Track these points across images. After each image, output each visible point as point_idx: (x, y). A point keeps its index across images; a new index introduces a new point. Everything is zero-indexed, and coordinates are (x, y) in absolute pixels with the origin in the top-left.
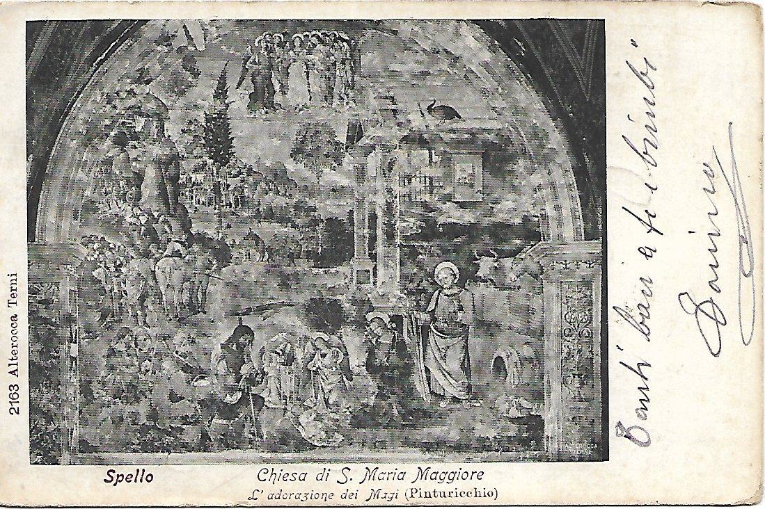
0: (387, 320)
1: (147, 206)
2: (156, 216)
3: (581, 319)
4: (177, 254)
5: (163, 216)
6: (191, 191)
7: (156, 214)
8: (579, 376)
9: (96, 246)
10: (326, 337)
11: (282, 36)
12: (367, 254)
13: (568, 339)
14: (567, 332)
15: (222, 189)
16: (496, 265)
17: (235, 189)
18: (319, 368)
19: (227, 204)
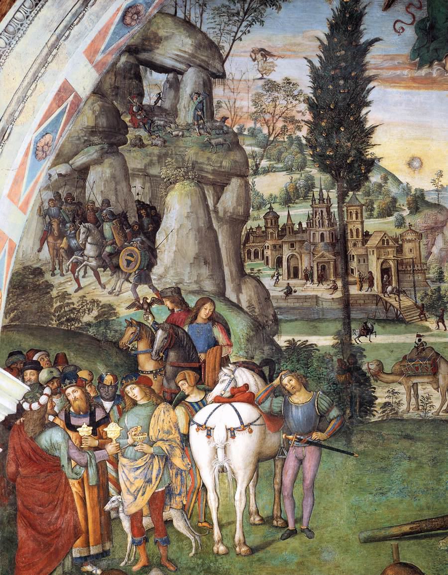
1: (170, 281)
2: (192, 305)
4: (240, 394)
5: (208, 306)
6: (277, 248)
7: (192, 301)
9: (44, 375)
15: (350, 245)
17: (384, 242)
19: (362, 280)
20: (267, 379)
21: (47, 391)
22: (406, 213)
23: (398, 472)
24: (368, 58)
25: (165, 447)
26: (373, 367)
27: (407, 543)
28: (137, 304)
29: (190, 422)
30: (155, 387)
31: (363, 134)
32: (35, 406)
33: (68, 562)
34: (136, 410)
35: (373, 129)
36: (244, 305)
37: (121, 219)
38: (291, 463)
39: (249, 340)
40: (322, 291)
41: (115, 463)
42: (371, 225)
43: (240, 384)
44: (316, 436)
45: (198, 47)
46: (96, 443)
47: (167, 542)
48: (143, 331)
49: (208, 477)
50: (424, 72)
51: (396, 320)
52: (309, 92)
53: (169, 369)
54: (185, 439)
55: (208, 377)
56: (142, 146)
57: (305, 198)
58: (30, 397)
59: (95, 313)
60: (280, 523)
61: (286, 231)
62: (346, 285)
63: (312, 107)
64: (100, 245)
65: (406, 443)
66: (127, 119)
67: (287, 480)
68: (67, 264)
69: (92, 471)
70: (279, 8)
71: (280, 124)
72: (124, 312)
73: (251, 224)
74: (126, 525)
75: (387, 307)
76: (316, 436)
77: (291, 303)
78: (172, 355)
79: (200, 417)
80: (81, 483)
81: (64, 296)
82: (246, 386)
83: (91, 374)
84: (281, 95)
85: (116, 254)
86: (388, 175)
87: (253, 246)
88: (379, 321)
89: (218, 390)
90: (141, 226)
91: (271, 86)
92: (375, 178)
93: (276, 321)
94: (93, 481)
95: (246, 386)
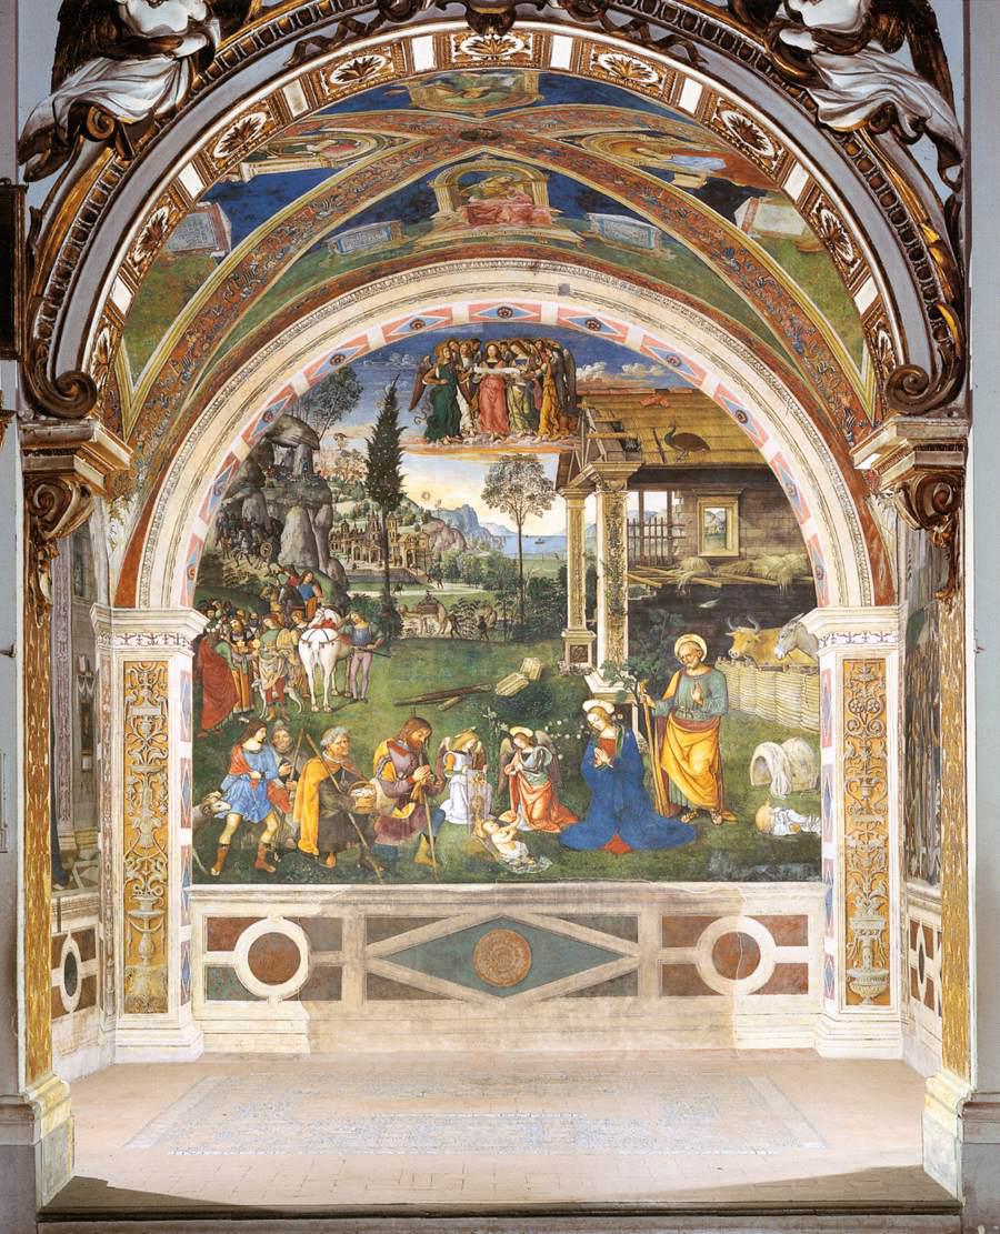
0: (610, 709)
1: (289, 561)
2: (300, 574)
3: (869, 708)
4: (326, 624)
6: (348, 543)
7: (300, 572)
8: (869, 781)
9: (218, 613)
10: (528, 732)
11: (471, 343)
12: (584, 623)
13: (853, 733)
14: (852, 725)
16: (756, 637)
18: (519, 772)
19: (396, 560)
20: (343, 616)
21: (220, 622)
22: (421, 523)
23: (416, 666)
24: (400, 437)
25: (285, 653)
26: (402, 609)
27: (419, 706)
28: (270, 574)
29: (299, 638)
30: (280, 620)
31: (397, 480)
32: (213, 630)
33: (231, 716)
34: (270, 632)
35: (402, 477)
36: (330, 575)
37: (261, 527)
38: (355, 662)
39: (332, 594)
40: (374, 567)
41: (257, 659)
42: (401, 530)
43: (327, 618)
44: (369, 647)
45: (305, 433)
46: (247, 650)
47: (286, 705)
48: (274, 590)
49: (308, 669)
50: (431, 445)
51: (415, 582)
52: (367, 457)
53: (288, 610)
54: (296, 648)
55: (310, 616)
56: (274, 487)
57: (365, 515)
58: (211, 625)
59: (247, 579)
60: (349, 695)
61: (355, 534)
62: (387, 563)
63: (368, 465)
64: (250, 543)
65: (420, 651)
66: (265, 473)
67: (353, 671)
68: (232, 552)
69: (244, 666)
70: (350, 411)
71: (350, 475)
72: (262, 578)
73: (333, 530)
74: (263, 695)
75: (410, 575)
76: (369, 647)
77: (356, 573)
78: (289, 601)
79: (305, 636)
80: (239, 673)
81: (230, 570)
82: (331, 619)
83: (244, 612)
84: (350, 458)
85: (258, 546)
86: (411, 502)
87: (334, 542)
88: (405, 583)
89: (315, 622)
90: (273, 530)
91: (346, 454)
92: (404, 504)
93: (348, 584)
94: (245, 672)
95: (331, 619)
